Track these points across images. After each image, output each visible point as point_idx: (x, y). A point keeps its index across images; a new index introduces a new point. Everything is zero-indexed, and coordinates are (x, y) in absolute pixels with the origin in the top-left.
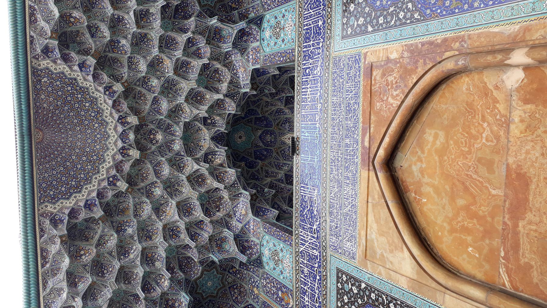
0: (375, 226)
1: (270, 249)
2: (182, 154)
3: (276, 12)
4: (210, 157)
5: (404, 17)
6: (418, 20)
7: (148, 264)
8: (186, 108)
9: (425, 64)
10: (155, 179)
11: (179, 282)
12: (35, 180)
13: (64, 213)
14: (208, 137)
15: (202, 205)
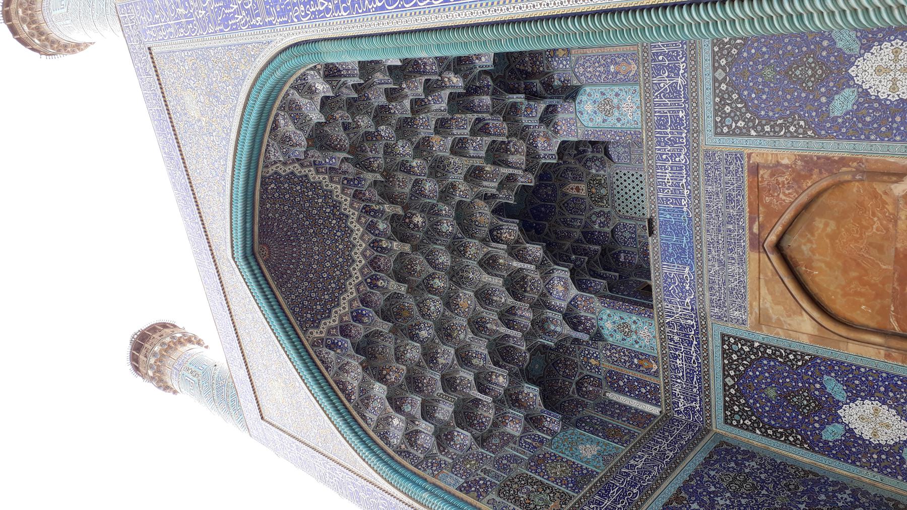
0: (769, 298)
1: (614, 322)
2: (460, 235)
3: (603, 89)
4: (495, 233)
5: (796, 131)
6: (812, 137)
7: (466, 365)
8: (462, 186)
9: (821, 173)
10: (431, 270)
11: (516, 374)
12: (285, 307)
13: (333, 335)
14: (487, 210)
15: (508, 289)
